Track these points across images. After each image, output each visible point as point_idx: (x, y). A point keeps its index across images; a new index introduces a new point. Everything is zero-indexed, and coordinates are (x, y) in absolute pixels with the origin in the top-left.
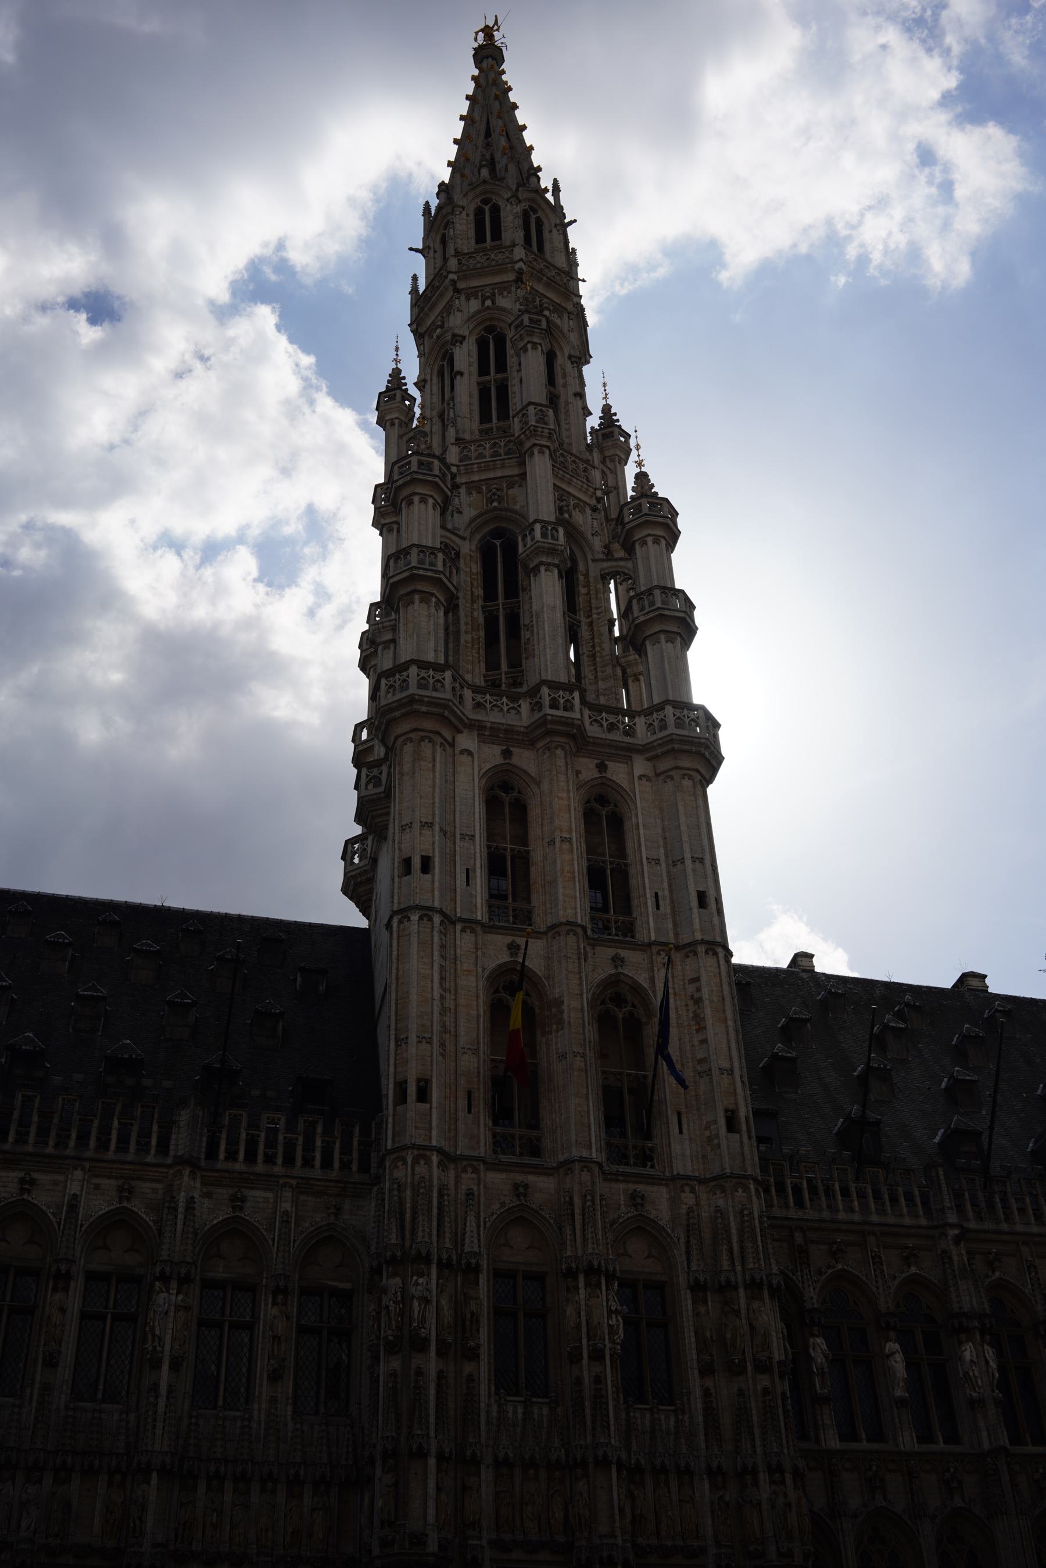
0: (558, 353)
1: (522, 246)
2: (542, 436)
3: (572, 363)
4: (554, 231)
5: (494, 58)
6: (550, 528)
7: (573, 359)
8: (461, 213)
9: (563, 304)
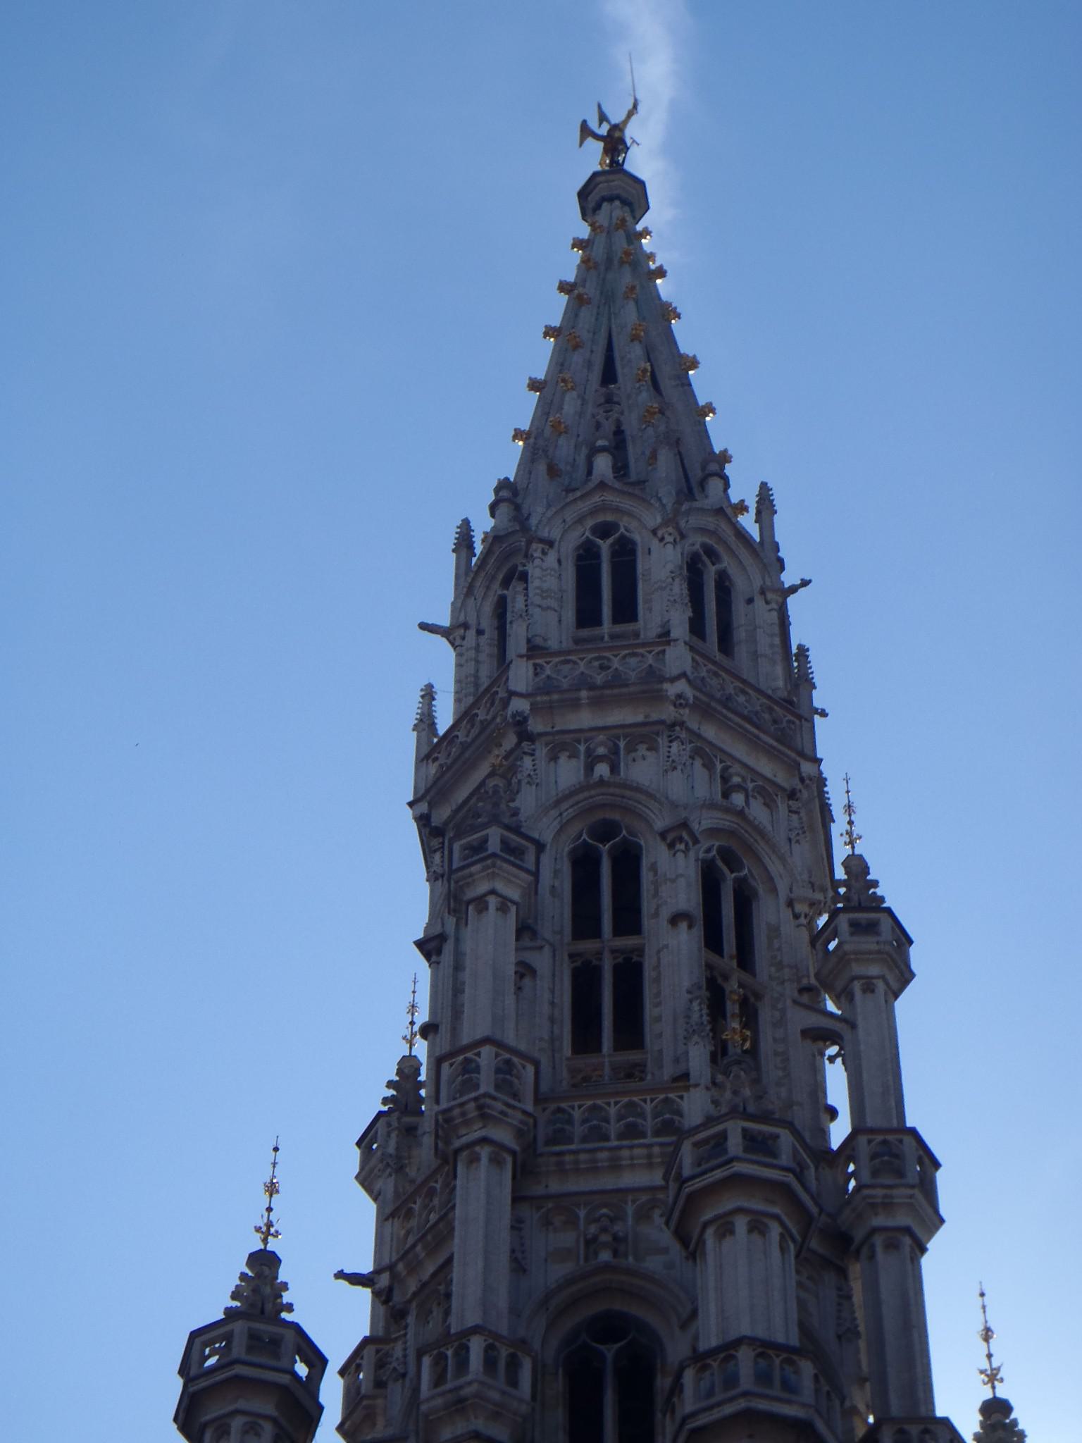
0: (642, 843)
1: (521, 656)
2: (467, 1123)
3: (671, 846)
4: (655, 544)
5: (610, 199)
6: (450, 1353)
7: (670, 837)
8: (463, 638)
9: (655, 717)
